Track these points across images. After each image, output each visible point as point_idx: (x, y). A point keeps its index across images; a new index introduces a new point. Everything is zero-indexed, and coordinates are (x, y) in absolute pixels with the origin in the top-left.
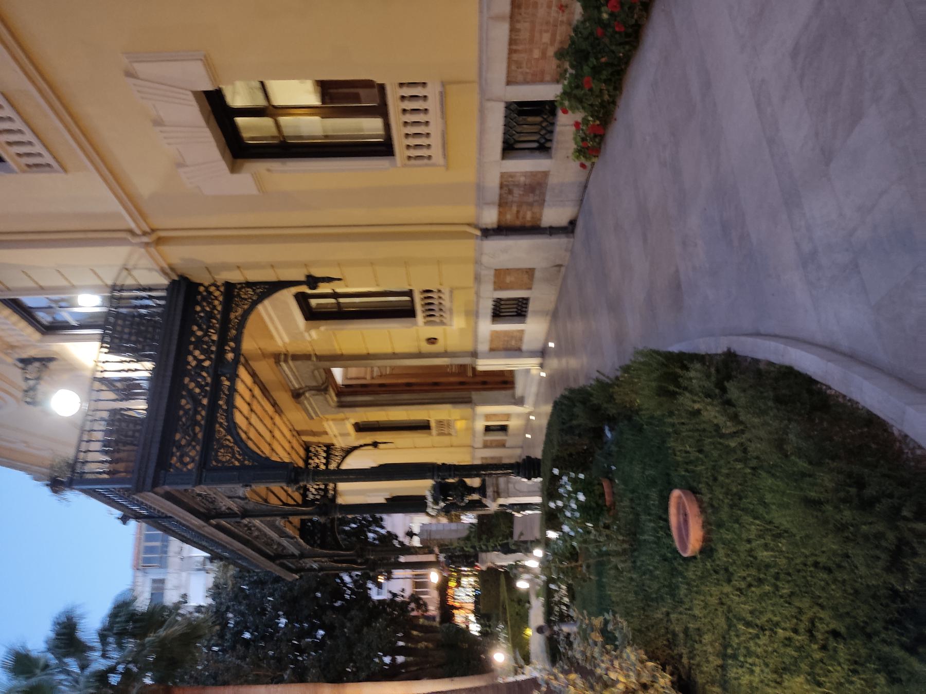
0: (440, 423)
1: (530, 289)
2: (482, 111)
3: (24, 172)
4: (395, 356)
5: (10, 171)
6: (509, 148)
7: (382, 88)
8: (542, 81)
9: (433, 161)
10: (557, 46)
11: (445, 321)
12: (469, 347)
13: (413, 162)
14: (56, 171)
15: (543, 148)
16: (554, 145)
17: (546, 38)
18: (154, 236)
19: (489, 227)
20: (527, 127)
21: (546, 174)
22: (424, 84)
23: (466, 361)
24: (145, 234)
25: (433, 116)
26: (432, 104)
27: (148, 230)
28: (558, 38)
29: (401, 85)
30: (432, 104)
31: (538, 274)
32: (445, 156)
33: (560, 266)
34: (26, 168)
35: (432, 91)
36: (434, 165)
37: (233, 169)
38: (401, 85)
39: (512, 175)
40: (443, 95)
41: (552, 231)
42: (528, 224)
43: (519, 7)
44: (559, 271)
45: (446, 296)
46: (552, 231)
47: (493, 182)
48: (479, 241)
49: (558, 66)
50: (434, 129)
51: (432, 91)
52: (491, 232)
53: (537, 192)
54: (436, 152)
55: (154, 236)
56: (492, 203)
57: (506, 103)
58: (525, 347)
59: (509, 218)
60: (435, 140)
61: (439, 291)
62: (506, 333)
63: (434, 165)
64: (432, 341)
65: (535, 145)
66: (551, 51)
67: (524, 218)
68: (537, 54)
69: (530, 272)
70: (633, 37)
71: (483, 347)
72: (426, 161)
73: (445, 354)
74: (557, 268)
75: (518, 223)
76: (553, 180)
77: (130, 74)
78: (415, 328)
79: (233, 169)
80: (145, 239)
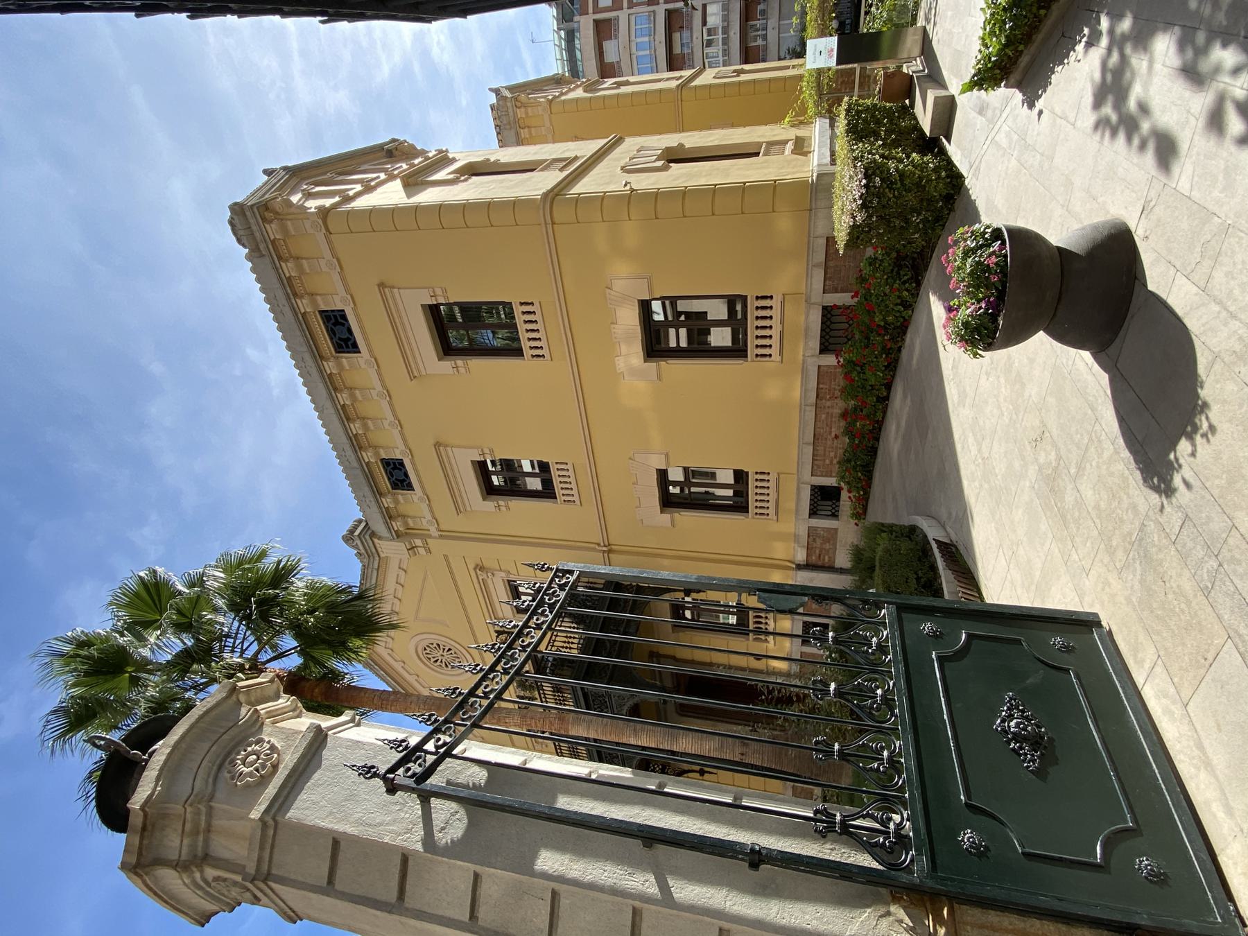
2: (798, 489)
6: (813, 513)
7: (747, 473)
15: (834, 516)
17: (832, 454)
20: (823, 500)
21: (836, 530)
25: (772, 491)
26: (772, 484)
32: (777, 513)
35: (772, 477)
37: (662, 512)
39: (816, 529)
40: (778, 480)
47: (803, 533)
50: (772, 498)
51: (772, 477)
66: (835, 461)
68: (827, 462)
70: (873, 452)
75: (820, 563)
76: (840, 534)
79: (662, 512)
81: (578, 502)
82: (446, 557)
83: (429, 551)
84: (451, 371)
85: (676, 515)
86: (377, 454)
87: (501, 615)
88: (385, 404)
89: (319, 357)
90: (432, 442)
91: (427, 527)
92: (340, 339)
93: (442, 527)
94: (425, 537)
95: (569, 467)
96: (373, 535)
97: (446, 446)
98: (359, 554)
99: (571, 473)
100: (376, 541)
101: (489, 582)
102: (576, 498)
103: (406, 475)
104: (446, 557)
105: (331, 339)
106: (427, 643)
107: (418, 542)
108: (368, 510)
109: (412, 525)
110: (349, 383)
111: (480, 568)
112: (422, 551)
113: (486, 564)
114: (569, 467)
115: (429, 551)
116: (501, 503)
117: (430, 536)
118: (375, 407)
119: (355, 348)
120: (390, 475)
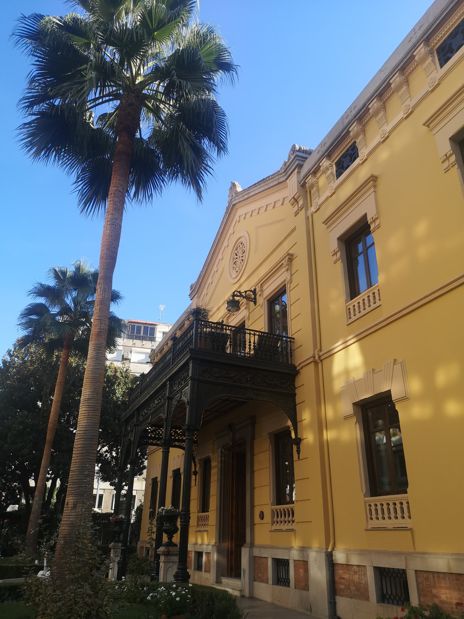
0: (207, 518)
1: (295, 588)
3: (346, 307)
4: (253, 489)
5: (346, 302)
6: (381, 572)
8: (419, 596)
9: (370, 521)
10: (440, 605)
11: (274, 525)
12: (258, 541)
13: (368, 507)
14: (348, 321)
16: (385, 605)
18: (319, 361)
19: (334, 558)
21: (367, 599)
22: (410, 517)
23: (248, 540)
24: (320, 357)
26: (400, 522)
27: (322, 358)
28: (444, 605)
29: (408, 503)
30: (400, 522)
31: (305, 593)
32: (374, 529)
33: (311, 610)
34: (348, 308)
36: (367, 521)
38: (408, 503)
40: (404, 529)
41: (333, 604)
42: (337, 587)
43: (457, 579)
44: (307, 610)
45: (290, 526)
46: (333, 604)
48: (324, 550)
49: (429, 606)
51: (406, 523)
52: (331, 559)
53: (356, 593)
54: (375, 523)
55: (319, 361)
56: (348, 561)
57: (406, 570)
58: (256, 584)
59: (339, 572)
60: (381, 523)
61: (293, 522)
62: (267, 570)
63: (367, 521)
64: (262, 516)
65: (385, 592)
67: (341, 583)
69: (306, 588)
71: (256, 552)
72: (369, 516)
73: (253, 525)
74: (309, 608)
75: (337, 578)
77: (395, 361)
78: (270, 503)
79: (355, 404)
80: (317, 357)
81: (350, 321)
82: (294, 229)
83: (296, 214)
84: (442, 155)
85: (354, 420)
86: (357, 135)
87: (264, 288)
88: (401, 115)
89: (427, 39)
90: (376, 174)
91: (314, 204)
92: (451, 44)
93: (315, 216)
94: (305, 206)
95: (378, 303)
96: (300, 166)
97: (375, 186)
98: (285, 163)
99: (373, 306)
100: (296, 170)
101: (284, 269)
102: (353, 318)
103: (348, 166)
104: (294, 229)
105: (449, 37)
106: (244, 242)
107: (301, 203)
108: (316, 152)
109: (312, 192)
110: (411, 79)
111: (290, 258)
112: (296, 208)
113: (295, 262)
114: (378, 303)
115: (296, 214)
116: (339, 254)
117: (307, 210)
118: (397, 109)
119: (443, 61)
120: (344, 156)
